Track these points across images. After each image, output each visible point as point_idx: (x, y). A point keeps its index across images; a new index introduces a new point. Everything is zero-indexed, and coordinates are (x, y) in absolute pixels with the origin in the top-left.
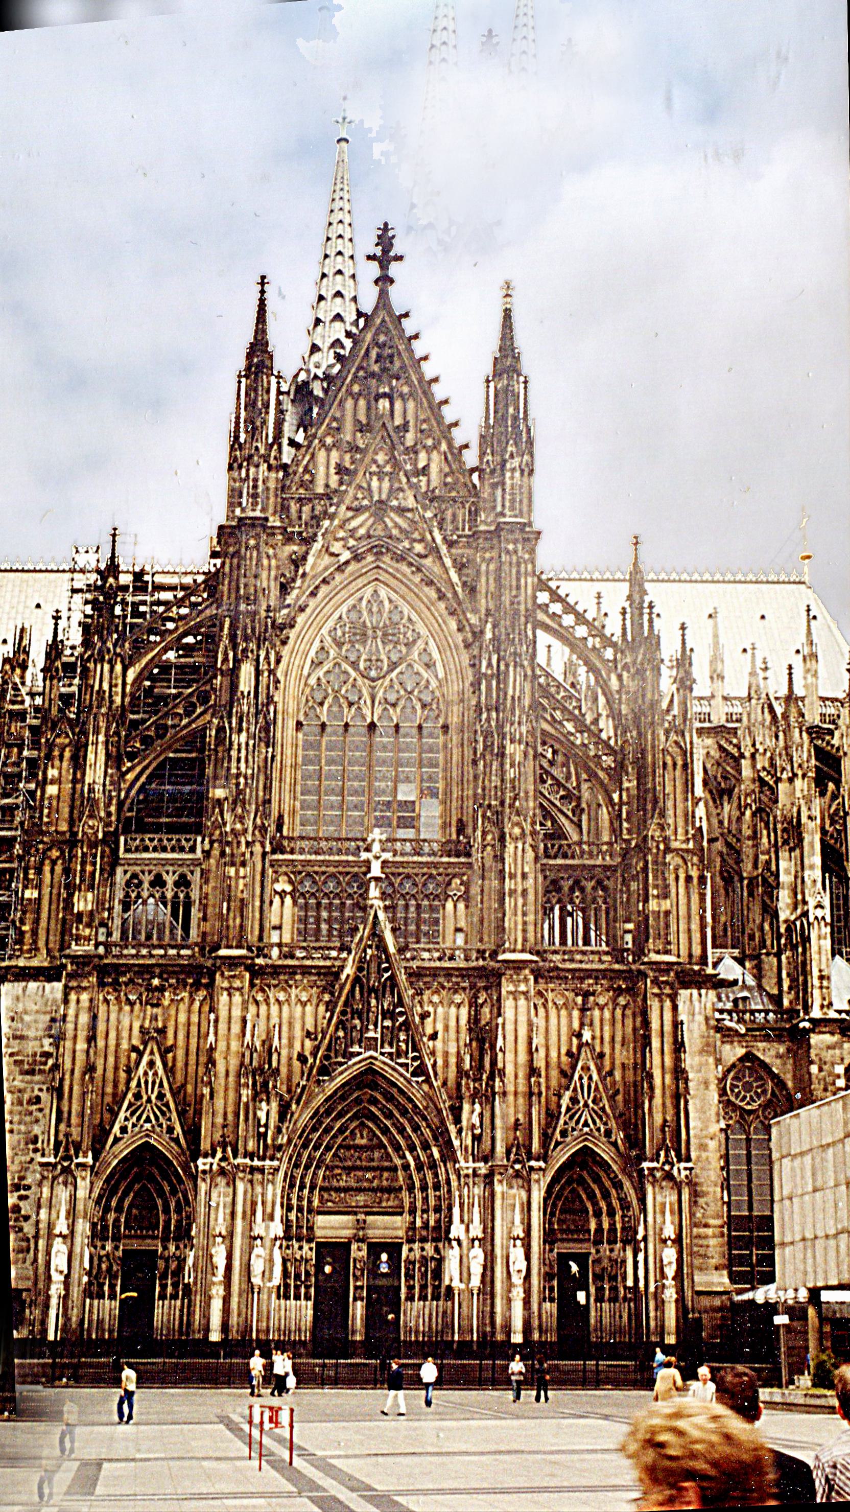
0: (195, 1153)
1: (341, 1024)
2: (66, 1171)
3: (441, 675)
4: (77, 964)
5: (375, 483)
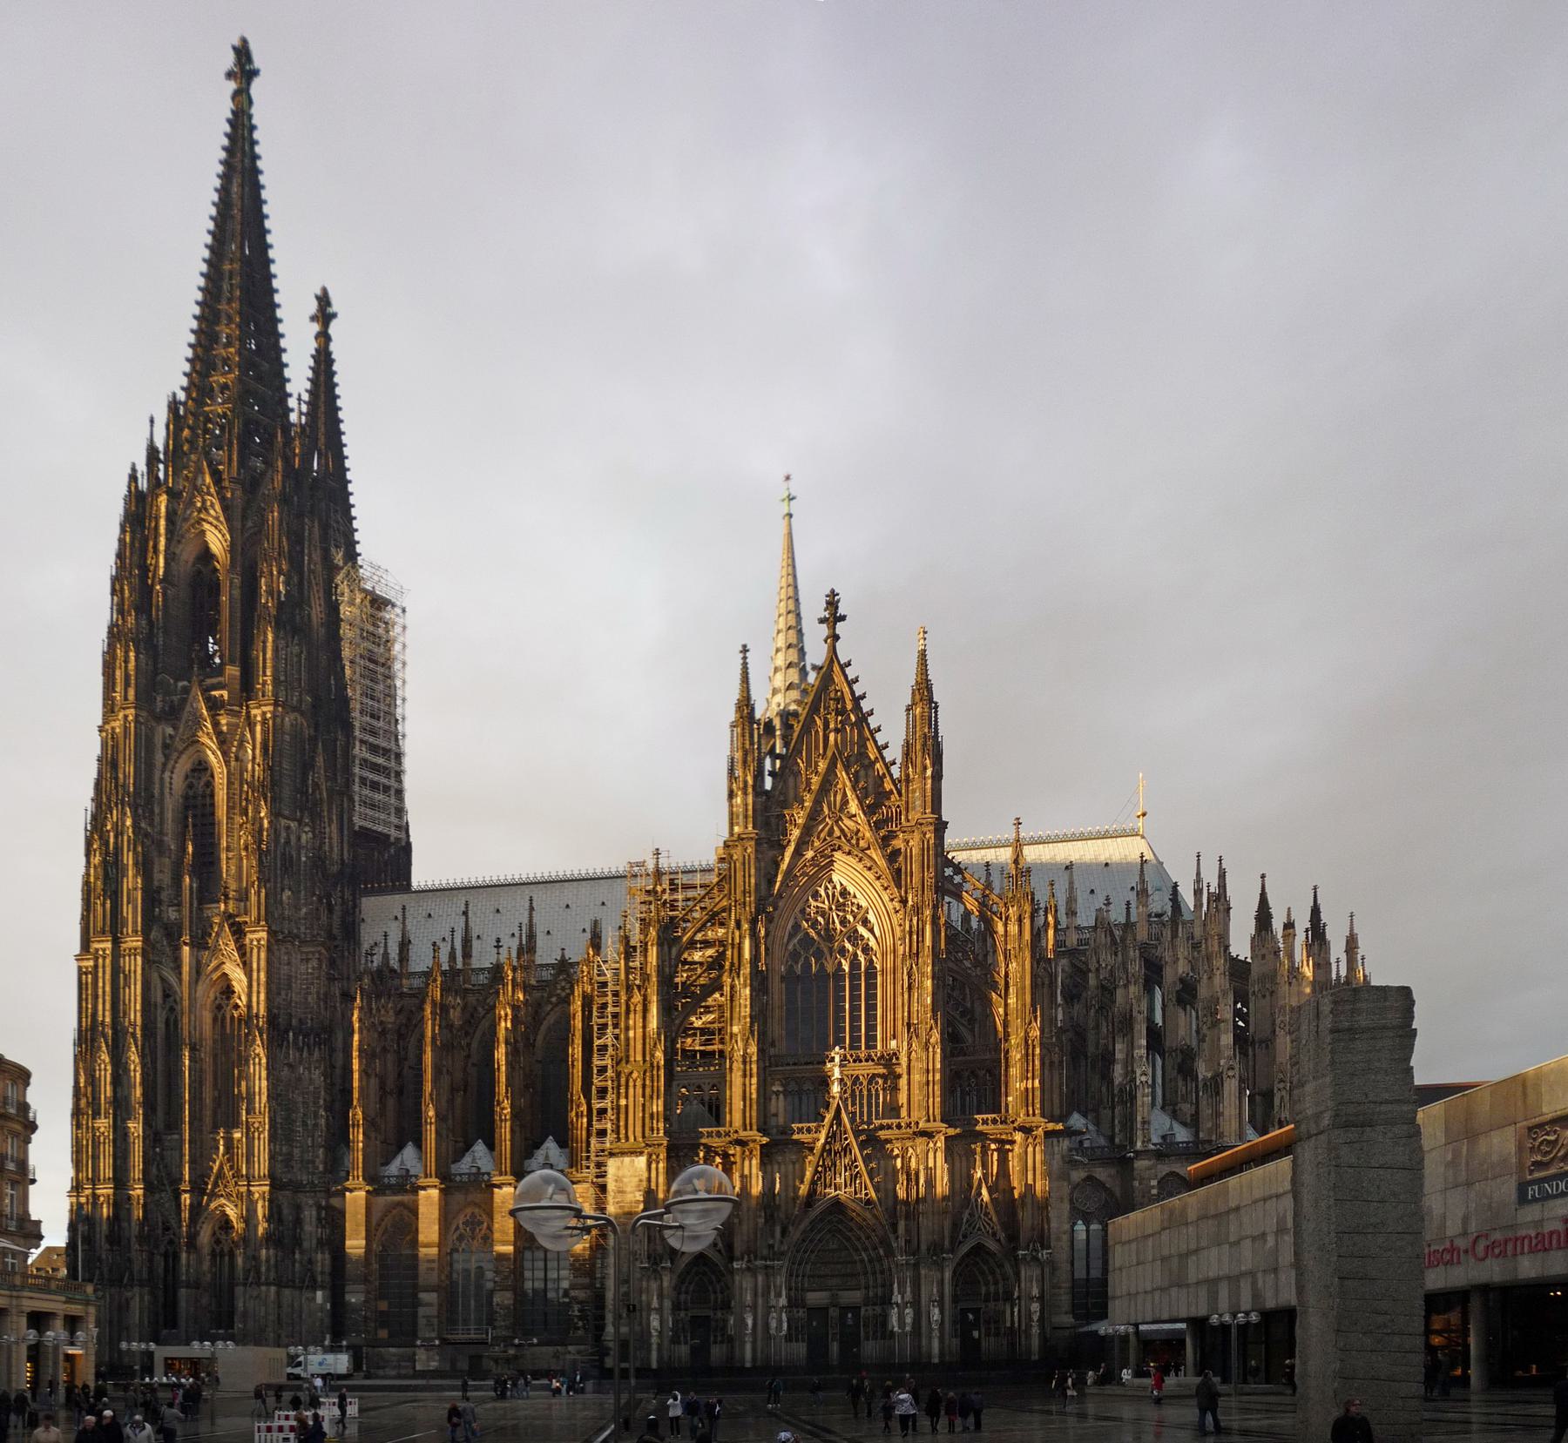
0: (732, 1259)
2: (655, 1271)
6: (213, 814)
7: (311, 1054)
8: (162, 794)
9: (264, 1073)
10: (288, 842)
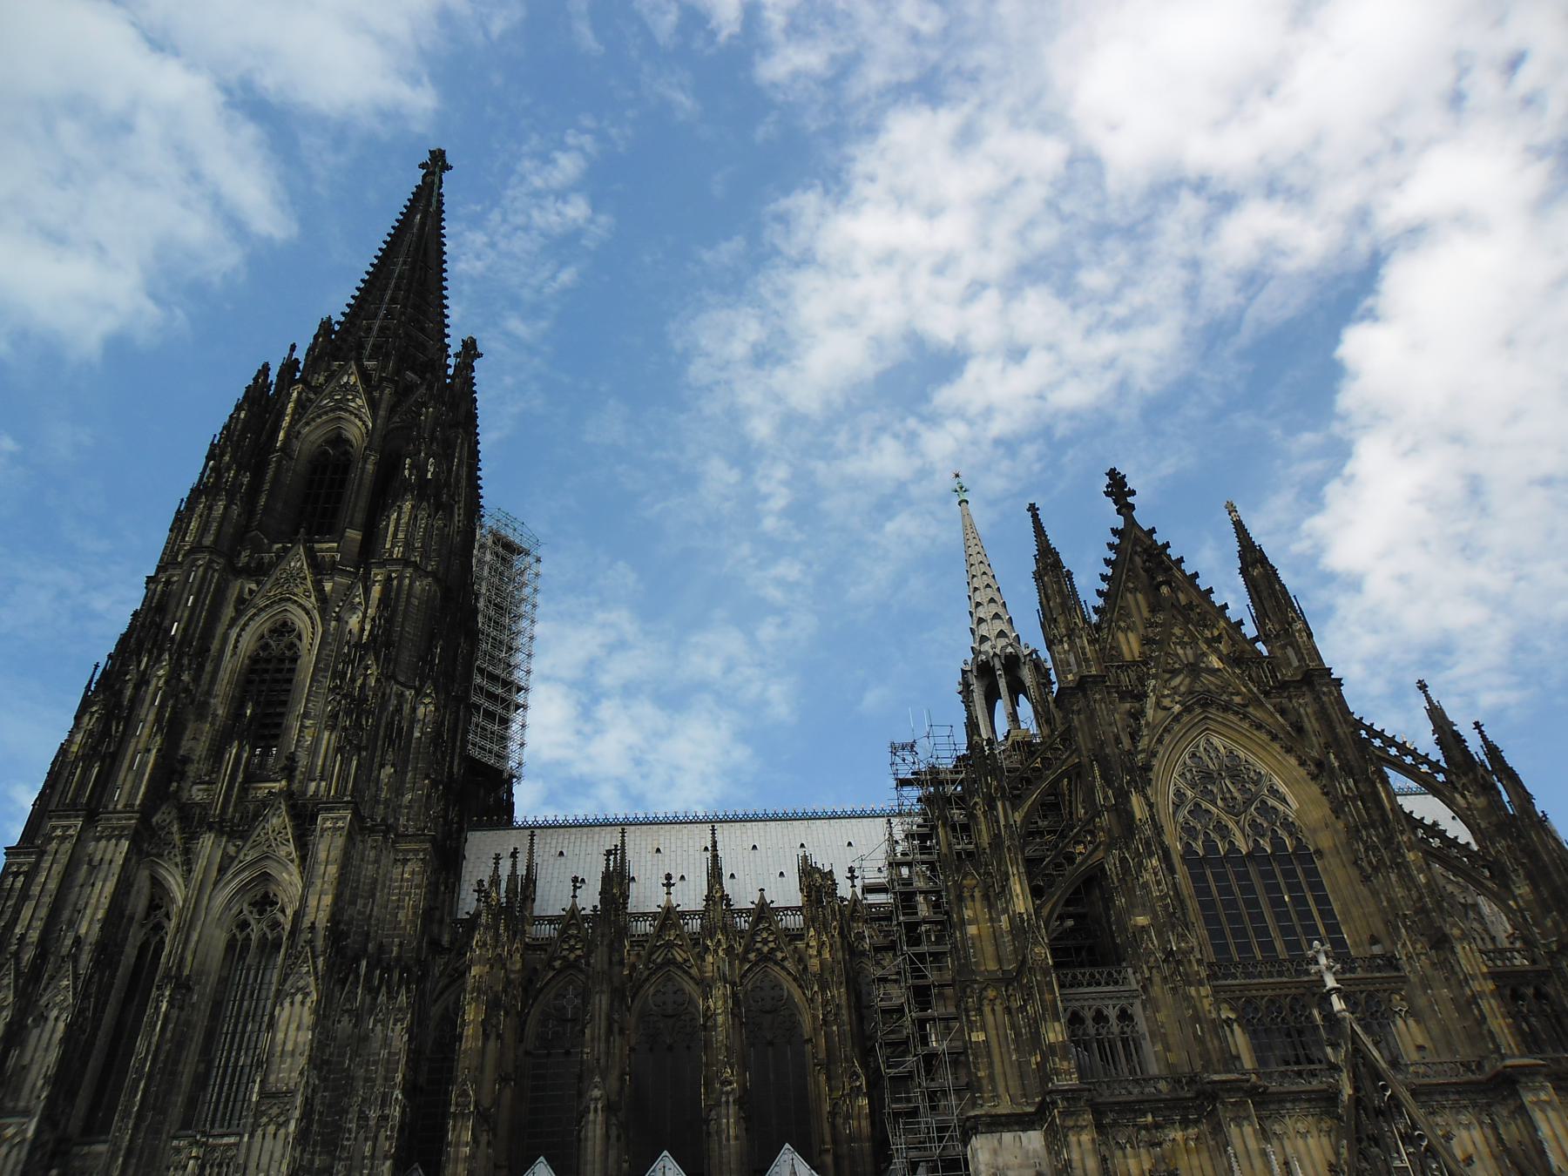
1: (1363, 1155)
3: (1295, 805)
4: (1067, 1100)
5: (1180, 651)
6: (290, 681)
7: (391, 996)
8: (222, 651)
9: (308, 1019)
10: (399, 710)
